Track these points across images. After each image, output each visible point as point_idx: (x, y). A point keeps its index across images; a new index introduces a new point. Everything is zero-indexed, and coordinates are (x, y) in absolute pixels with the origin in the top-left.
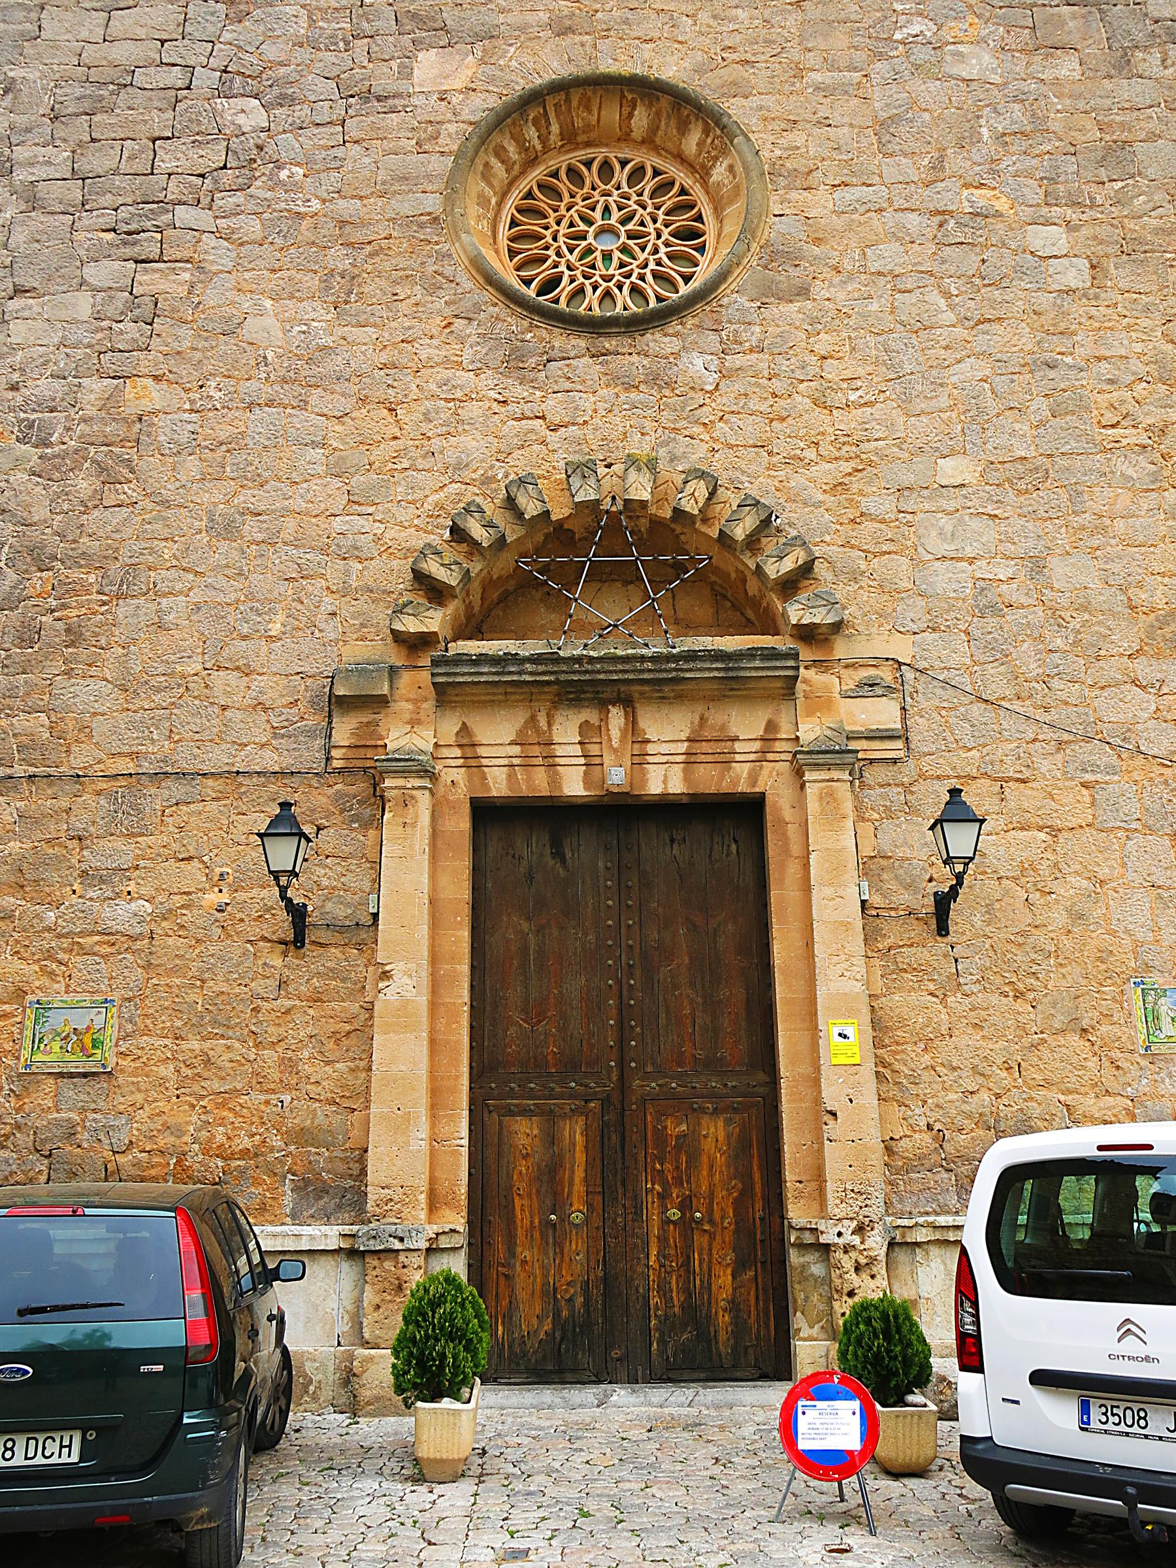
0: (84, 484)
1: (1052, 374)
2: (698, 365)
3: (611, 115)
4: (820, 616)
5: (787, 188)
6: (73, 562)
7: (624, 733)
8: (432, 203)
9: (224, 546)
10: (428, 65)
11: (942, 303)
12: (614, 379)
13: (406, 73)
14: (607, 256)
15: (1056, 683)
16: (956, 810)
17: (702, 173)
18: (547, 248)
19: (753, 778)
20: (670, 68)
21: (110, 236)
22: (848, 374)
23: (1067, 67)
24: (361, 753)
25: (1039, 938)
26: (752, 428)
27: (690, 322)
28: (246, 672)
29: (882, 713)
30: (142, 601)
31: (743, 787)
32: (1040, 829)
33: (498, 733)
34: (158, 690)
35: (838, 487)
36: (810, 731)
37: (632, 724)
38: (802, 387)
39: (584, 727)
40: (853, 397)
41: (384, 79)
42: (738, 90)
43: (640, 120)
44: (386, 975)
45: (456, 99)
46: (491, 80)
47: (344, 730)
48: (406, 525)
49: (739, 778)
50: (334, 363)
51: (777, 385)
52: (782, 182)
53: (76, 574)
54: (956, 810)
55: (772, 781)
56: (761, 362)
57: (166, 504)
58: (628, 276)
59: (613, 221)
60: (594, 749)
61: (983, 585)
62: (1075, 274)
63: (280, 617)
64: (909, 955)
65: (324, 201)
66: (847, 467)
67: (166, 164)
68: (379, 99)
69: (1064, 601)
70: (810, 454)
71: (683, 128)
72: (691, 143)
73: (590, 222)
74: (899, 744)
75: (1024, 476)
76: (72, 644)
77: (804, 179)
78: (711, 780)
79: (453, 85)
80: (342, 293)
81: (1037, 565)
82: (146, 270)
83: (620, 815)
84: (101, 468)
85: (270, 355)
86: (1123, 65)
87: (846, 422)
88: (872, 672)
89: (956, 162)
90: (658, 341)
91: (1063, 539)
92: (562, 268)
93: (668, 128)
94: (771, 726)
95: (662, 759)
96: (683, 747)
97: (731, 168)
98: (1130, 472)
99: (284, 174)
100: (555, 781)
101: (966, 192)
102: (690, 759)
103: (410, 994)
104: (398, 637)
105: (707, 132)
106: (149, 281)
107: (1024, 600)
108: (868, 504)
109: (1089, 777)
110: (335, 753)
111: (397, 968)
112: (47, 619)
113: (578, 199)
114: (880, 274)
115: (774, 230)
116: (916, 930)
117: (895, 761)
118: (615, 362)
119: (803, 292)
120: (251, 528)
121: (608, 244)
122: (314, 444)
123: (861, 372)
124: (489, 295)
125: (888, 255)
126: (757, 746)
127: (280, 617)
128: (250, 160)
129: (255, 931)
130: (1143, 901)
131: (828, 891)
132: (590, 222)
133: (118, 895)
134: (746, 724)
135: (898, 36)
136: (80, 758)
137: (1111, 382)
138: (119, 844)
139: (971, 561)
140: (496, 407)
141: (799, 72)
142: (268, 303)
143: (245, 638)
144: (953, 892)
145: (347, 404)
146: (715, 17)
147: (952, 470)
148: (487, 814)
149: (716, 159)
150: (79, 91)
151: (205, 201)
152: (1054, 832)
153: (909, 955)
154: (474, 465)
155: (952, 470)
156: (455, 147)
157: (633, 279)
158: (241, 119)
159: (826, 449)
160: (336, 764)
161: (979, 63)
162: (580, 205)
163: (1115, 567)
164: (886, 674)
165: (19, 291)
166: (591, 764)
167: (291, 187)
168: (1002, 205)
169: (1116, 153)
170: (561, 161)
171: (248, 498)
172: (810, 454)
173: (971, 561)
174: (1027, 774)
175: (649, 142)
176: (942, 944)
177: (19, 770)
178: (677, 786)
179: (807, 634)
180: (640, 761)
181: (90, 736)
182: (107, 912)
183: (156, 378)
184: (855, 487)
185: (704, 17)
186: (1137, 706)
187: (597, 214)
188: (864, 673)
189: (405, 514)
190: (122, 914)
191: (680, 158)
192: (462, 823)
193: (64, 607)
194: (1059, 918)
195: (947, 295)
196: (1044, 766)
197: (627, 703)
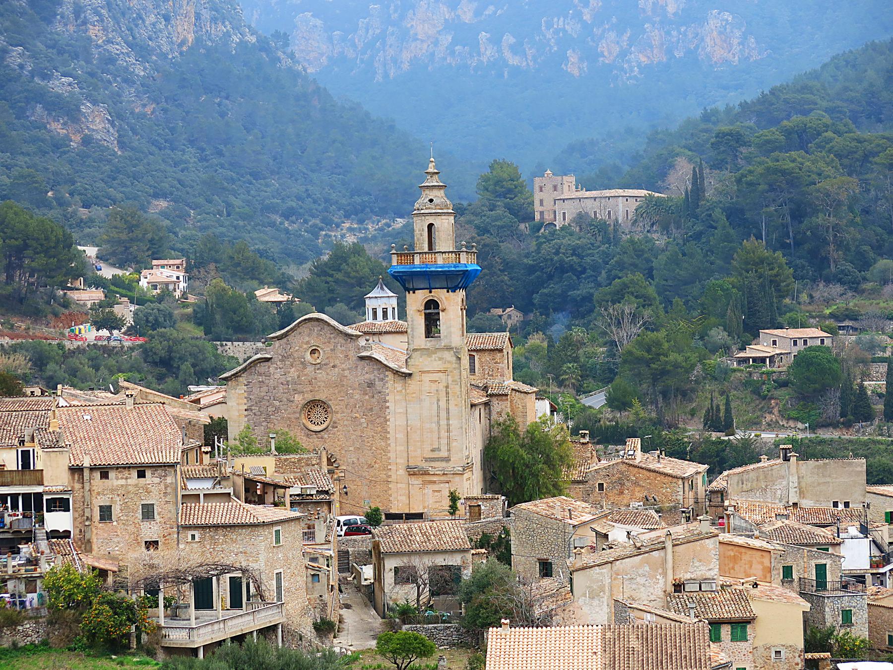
2: (326, 436)
8: (298, 415)
20: (323, 398)
23: (367, 397)
36: (335, 476)
77: (337, 413)
79: (299, 399)
86: (373, 397)
89: (354, 410)
125: (346, 423)
128: (277, 409)
147: (351, 448)
155: (351, 448)
161: (357, 397)
169: (371, 410)
186: (367, 474)
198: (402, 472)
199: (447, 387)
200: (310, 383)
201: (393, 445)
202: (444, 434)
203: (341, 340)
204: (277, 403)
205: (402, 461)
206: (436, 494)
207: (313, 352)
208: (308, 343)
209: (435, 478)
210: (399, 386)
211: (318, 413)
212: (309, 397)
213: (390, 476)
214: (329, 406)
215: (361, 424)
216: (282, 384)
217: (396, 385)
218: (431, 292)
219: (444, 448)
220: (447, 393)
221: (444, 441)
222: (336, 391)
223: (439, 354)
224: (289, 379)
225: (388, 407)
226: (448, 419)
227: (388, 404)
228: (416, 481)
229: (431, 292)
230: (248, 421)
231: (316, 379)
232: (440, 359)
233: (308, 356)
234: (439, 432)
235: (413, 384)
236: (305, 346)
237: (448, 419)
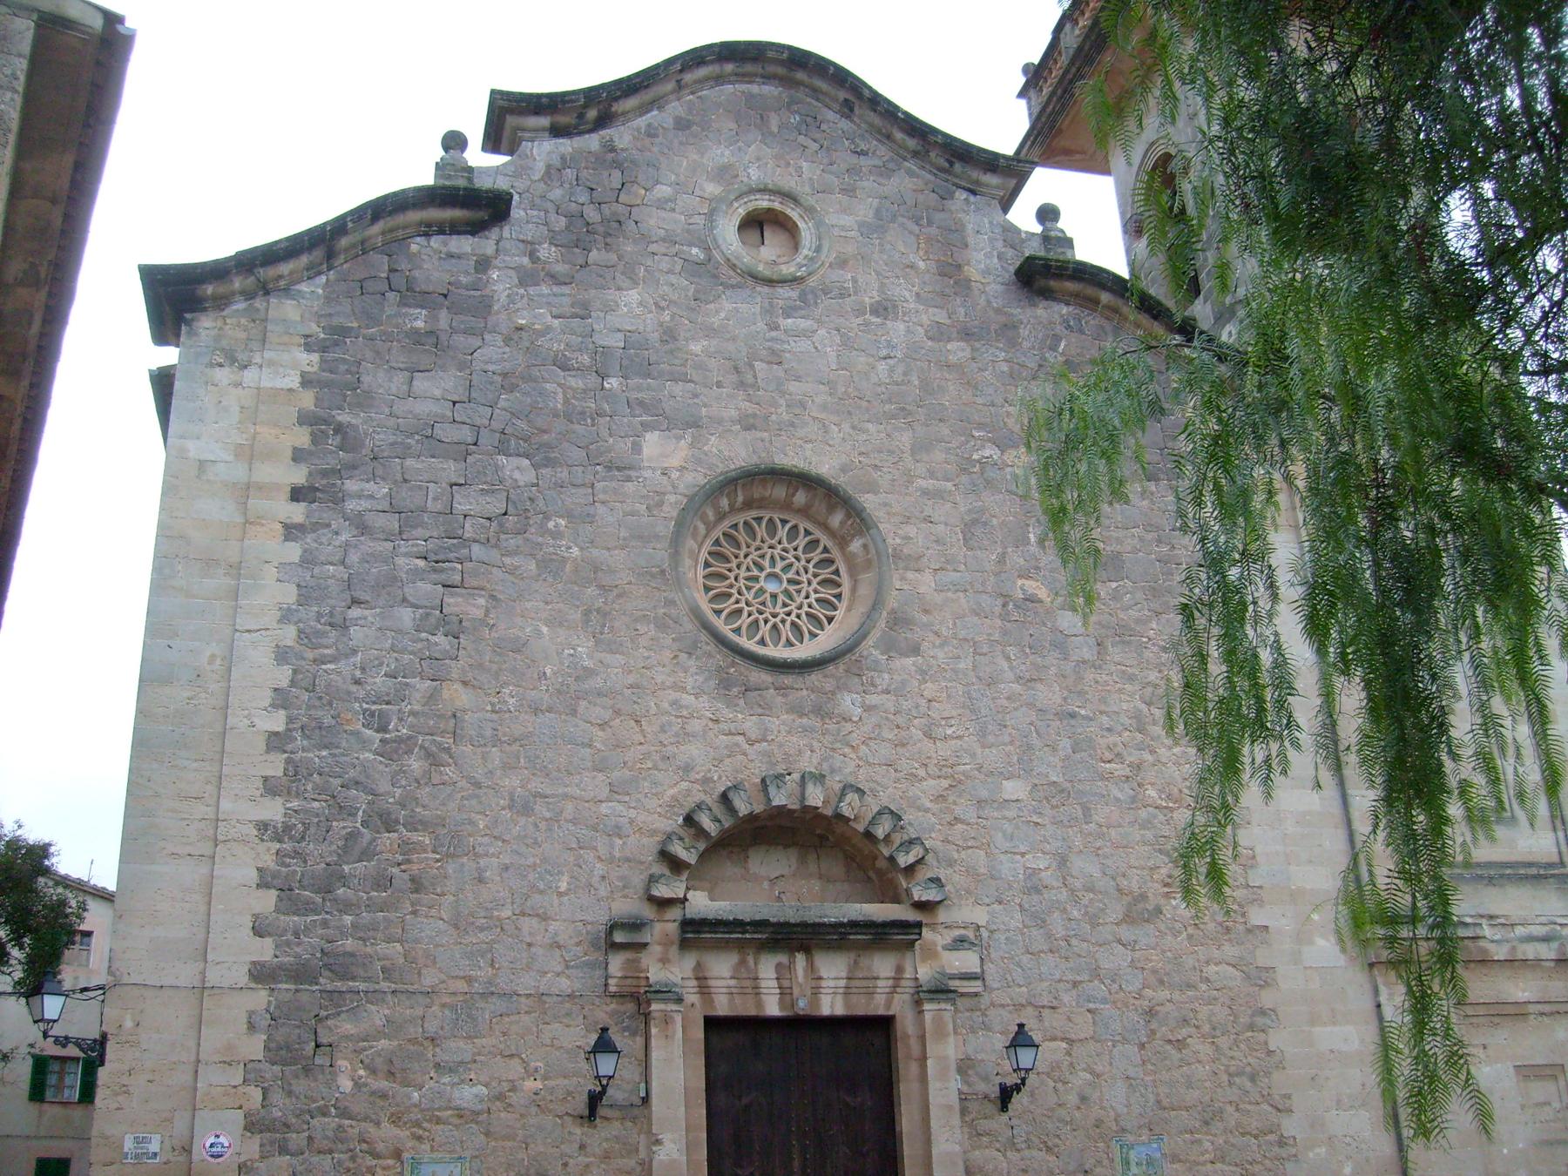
0: (415, 764)
1: (1073, 722)
3: (780, 492)
4: (931, 895)
5: (906, 569)
6: (412, 826)
7: (805, 971)
9: (522, 820)
10: (652, 443)
11: (1005, 665)
13: (637, 449)
14: (774, 596)
15: (1074, 942)
16: (1021, 1039)
17: (843, 543)
18: (731, 586)
19: (889, 1004)
20: (824, 466)
21: (421, 563)
22: (946, 714)
24: (629, 981)
25: (1062, 1112)
26: (885, 751)
27: (842, 667)
28: (544, 918)
29: (967, 961)
30: (465, 859)
31: (881, 1012)
32: (1062, 1040)
33: (721, 967)
34: (482, 929)
35: (940, 798)
36: (925, 972)
37: (811, 966)
38: (916, 722)
39: (779, 966)
40: (949, 732)
42: (873, 488)
43: (800, 498)
44: (658, 1142)
45: (675, 475)
46: (699, 461)
47: (616, 963)
48: (652, 815)
49: (878, 1007)
50: (597, 683)
51: (900, 720)
52: (901, 564)
53: (415, 837)
54: (1021, 1039)
55: (900, 1007)
56: (888, 702)
57: (478, 785)
58: (789, 614)
59: (777, 570)
60: (786, 983)
61: (1032, 873)
62: (1088, 653)
63: (565, 878)
64: (984, 1125)
65: (582, 549)
66: (945, 783)
67: (461, 506)
68: (619, 469)
69: (1078, 884)
70: (922, 773)
71: (831, 509)
72: (836, 520)
73: (761, 569)
74: (979, 983)
75: (1052, 794)
76: (417, 891)
77: (914, 562)
78: (862, 1009)
79: (670, 462)
81: (1063, 861)
82: (452, 595)
83: (800, 1026)
84: (429, 755)
85: (548, 671)
87: (944, 750)
88: (962, 932)
91: (1078, 843)
92: (742, 605)
93: (820, 507)
94: (900, 969)
95: (830, 985)
96: (843, 983)
97: (865, 546)
98: (1119, 795)
99: (551, 525)
100: (759, 1004)
101: (1020, 582)
102: (847, 992)
103: (675, 1156)
104: (652, 899)
105: (848, 516)
106: (454, 603)
107: (1055, 884)
108: (958, 811)
109: (1091, 1006)
110: (611, 981)
111: (666, 1137)
112: (395, 870)
113: (752, 549)
114: (966, 640)
115: (892, 601)
116: (991, 1108)
117: (976, 995)
118: (793, 696)
119: (915, 650)
120: (541, 809)
121: (772, 587)
122: (583, 745)
123: (954, 713)
124: (704, 637)
126: (891, 982)
127: (565, 878)
129: (561, 1109)
130: (1121, 1088)
131: (938, 1085)
132: (761, 569)
133: (463, 1081)
134: (882, 965)
135: (975, 457)
136: (429, 979)
137: (1109, 730)
138: (461, 1044)
139: (1023, 855)
140: (711, 724)
141: (910, 478)
142: (545, 629)
143: (541, 892)
144: (1017, 1088)
145: (607, 715)
146: (853, 428)
148: (713, 1024)
149: (853, 536)
150: (392, 438)
151: (493, 541)
152: (1070, 1042)
153: (984, 1125)
154: (698, 768)
155: (1014, 789)
156: (675, 514)
157: (793, 617)
158: (517, 475)
159: (933, 770)
160: (612, 989)
162: (754, 555)
163: (1109, 862)
164: (970, 934)
165: (356, 602)
166: (785, 992)
167: (557, 535)
168: (1042, 593)
170: (740, 519)
171: (537, 784)
172: (922, 773)
173: (1023, 855)
174: (1055, 1003)
175: (804, 512)
176: (1005, 1117)
177: (384, 985)
178: (840, 1010)
179: (922, 906)
180: (816, 991)
181: (434, 962)
182: (456, 1094)
183: (465, 683)
184: (951, 799)
185: (846, 427)
187: (766, 563)
188: (957, 933)
189: (652, 803)
190: (468, 1095)
191: (825, 527)
192: (699, 1033)
193: (409, 861)
194: (1072, 1099)
195: (1008, 658)
196: (1066, 998)
197: (807, 950)
198: (1325, 950)
203: (908, 182)
207: (755, 224)
208: (723, 173)
209: (1521, 990)
211: (776, 572)
212: (738, 453)
213: (1262, 978)
214: (859, 520)
222: (905, 439)
224: (616, 341)
230: (308, 560)
231: (776, 359)
236: (712, 189)
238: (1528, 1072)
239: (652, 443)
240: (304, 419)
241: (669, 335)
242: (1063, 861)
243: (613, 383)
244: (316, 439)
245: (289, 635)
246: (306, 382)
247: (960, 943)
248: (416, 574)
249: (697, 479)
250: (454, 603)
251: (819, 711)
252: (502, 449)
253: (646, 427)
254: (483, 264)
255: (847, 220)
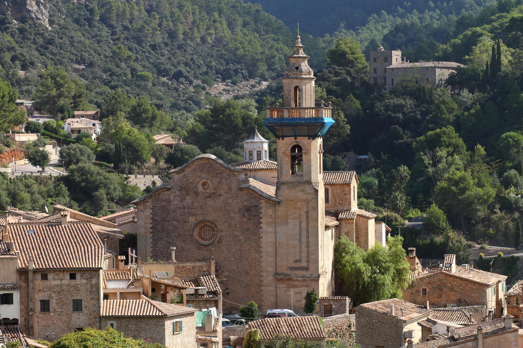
12: (207, 250)
29: (225, 279)
41: (187, 220)
42: (217, 221)
62: (243, 241)
80: (184, 241)
81: (238, 267)
90: (210, 247)
155: (233, 259)
168: (238, 234)
198: (271, 278)
199: (307, 213)
200: (201, 207)
201: (264, 257)
202: (304, 249)
204: (175, 223)
205: (271, 269)
206: (298, 295)
210: (270, 212)
212: (200, 218)
214: (216, 226)
215: (240, 240)
216: (180, 208)
217: (268, 211)
218: (296, 139)
219: (304, 260)
220: (307, 217)
221: (304, 255)
222: (222, 215)
223: (301, 187)
224: (185, 205)
225: (261, 228)
226: (308, 237)
227: (261, 225)
228: (282, 286)
229: (296, 139)
231: (206, 204)
232: (302, 191)
233: (200, 188)
234: (301, 247)
235: (281, 210)
237: (308, 237)
238: (296, 293)
239: (190, 218)
240: (151, 218)
241: (192, 203)
242: (238, 267)
243: (186, 210)
244: (153, 221)
245: (152, 245)
246: (151, 214)
247: (224, 277)
248: (165, 237)
249: (196, 222)
250: (169, 240)
251: (210, 250)
252: (173, 220)
253: (190, 216)
254: (170, 195)
255: (216, 182)
